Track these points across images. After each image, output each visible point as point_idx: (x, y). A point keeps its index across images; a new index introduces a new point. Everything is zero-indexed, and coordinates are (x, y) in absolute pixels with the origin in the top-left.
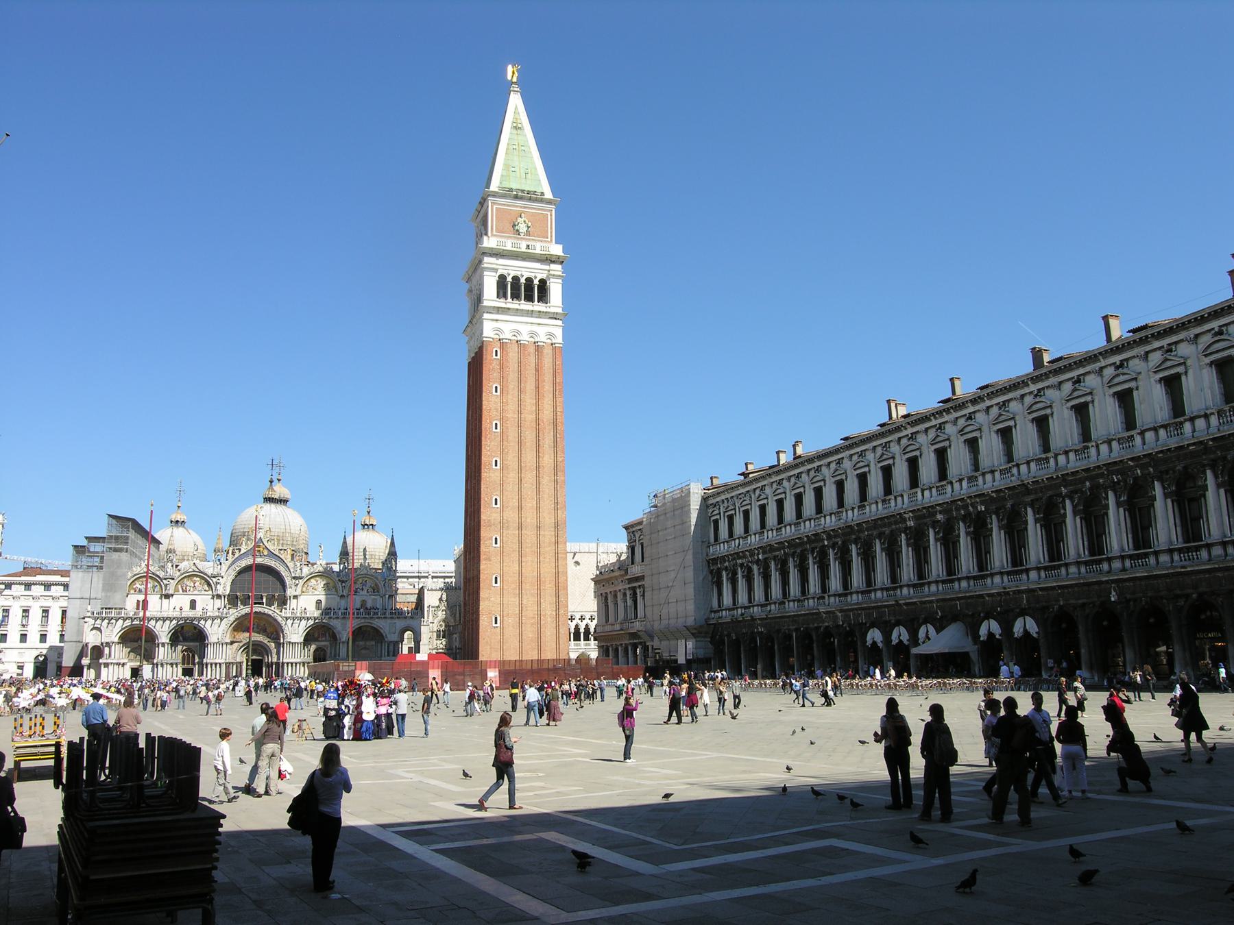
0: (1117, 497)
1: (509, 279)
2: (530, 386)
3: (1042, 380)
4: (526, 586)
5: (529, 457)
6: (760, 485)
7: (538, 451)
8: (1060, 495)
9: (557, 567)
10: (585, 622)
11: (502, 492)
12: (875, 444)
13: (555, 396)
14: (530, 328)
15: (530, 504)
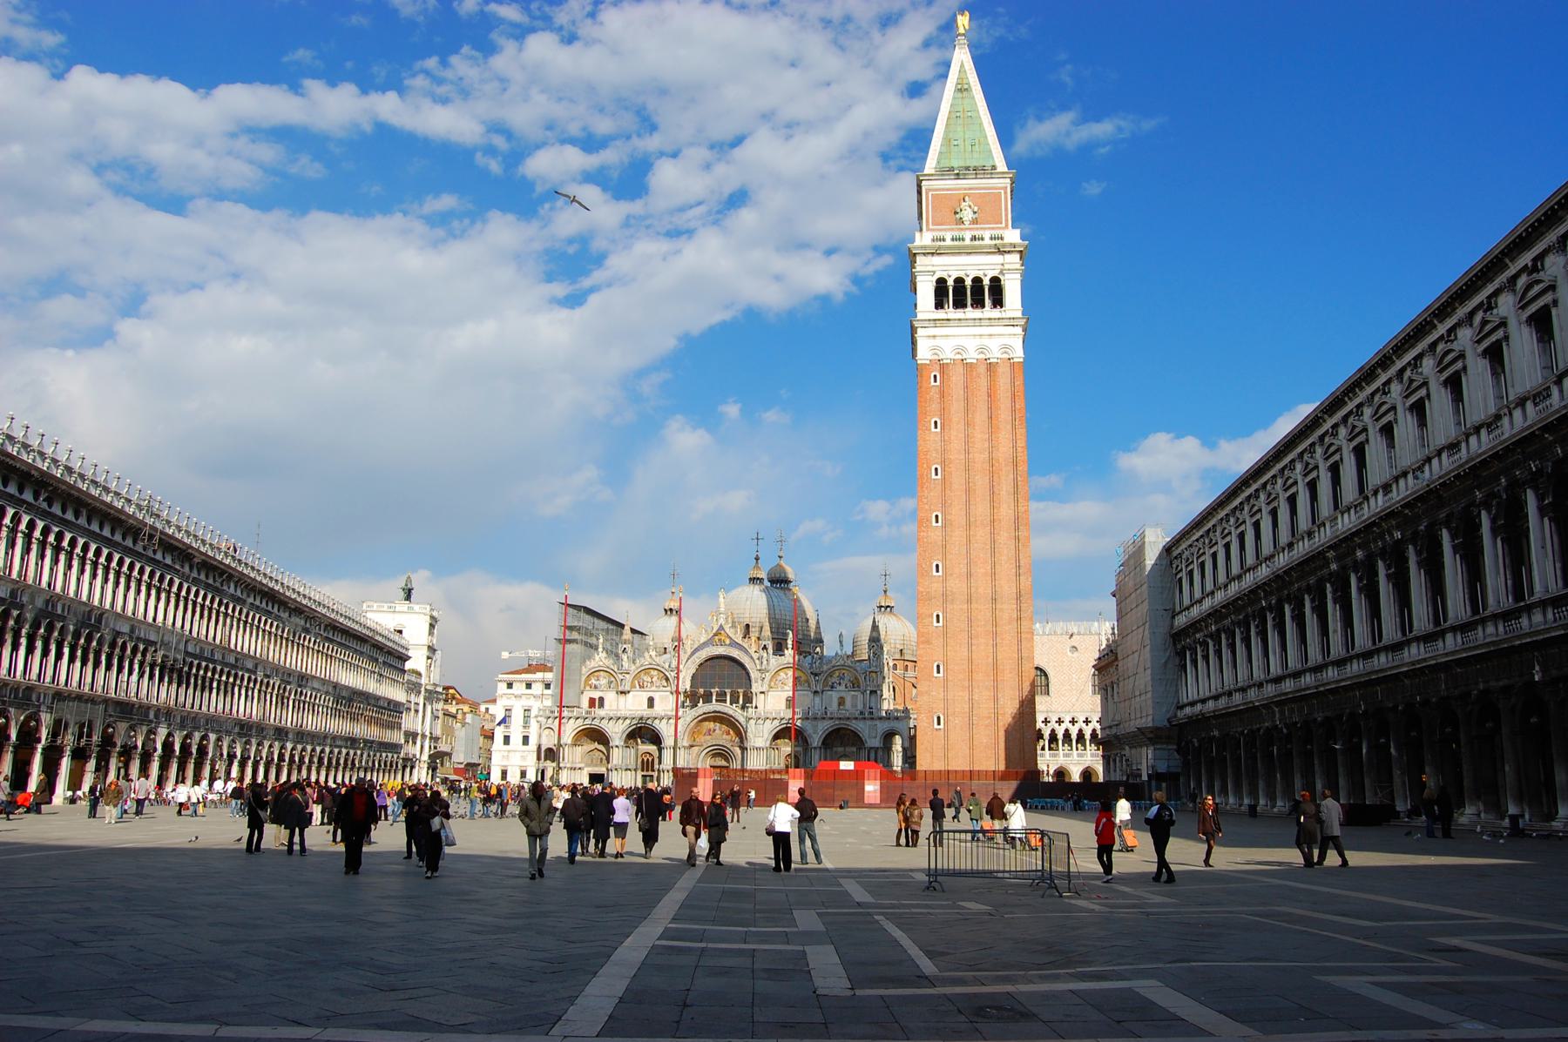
0: (1540, 498)
1: (950, 282)
2: (981, 417)
3: (1449, 315)
4: (978, 676)
5: (981, 509)
6: (1210, 525)
7: (992, 501)
8: (1472, 504)
9: (1020, 650)
10: (1064, 726)
11: (945, 555)
12: (1300, 449)
13: (1014, 428)
14: (978, 342)
15: (982, 570)
